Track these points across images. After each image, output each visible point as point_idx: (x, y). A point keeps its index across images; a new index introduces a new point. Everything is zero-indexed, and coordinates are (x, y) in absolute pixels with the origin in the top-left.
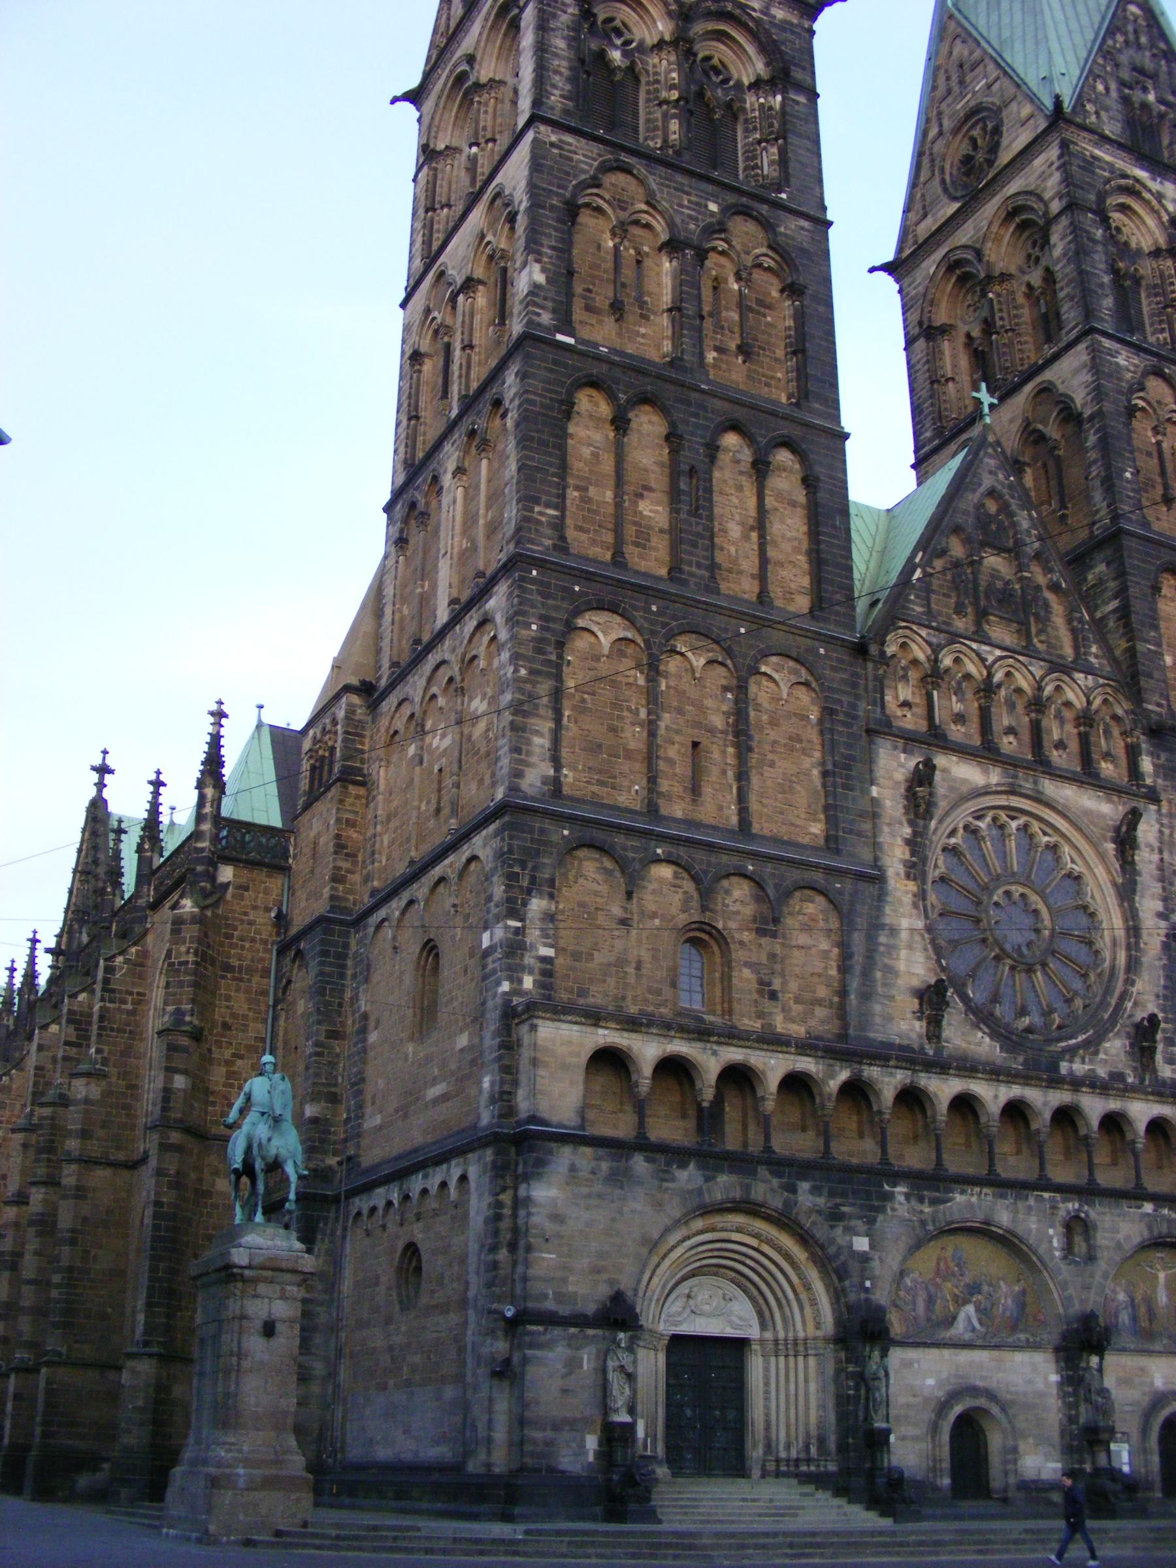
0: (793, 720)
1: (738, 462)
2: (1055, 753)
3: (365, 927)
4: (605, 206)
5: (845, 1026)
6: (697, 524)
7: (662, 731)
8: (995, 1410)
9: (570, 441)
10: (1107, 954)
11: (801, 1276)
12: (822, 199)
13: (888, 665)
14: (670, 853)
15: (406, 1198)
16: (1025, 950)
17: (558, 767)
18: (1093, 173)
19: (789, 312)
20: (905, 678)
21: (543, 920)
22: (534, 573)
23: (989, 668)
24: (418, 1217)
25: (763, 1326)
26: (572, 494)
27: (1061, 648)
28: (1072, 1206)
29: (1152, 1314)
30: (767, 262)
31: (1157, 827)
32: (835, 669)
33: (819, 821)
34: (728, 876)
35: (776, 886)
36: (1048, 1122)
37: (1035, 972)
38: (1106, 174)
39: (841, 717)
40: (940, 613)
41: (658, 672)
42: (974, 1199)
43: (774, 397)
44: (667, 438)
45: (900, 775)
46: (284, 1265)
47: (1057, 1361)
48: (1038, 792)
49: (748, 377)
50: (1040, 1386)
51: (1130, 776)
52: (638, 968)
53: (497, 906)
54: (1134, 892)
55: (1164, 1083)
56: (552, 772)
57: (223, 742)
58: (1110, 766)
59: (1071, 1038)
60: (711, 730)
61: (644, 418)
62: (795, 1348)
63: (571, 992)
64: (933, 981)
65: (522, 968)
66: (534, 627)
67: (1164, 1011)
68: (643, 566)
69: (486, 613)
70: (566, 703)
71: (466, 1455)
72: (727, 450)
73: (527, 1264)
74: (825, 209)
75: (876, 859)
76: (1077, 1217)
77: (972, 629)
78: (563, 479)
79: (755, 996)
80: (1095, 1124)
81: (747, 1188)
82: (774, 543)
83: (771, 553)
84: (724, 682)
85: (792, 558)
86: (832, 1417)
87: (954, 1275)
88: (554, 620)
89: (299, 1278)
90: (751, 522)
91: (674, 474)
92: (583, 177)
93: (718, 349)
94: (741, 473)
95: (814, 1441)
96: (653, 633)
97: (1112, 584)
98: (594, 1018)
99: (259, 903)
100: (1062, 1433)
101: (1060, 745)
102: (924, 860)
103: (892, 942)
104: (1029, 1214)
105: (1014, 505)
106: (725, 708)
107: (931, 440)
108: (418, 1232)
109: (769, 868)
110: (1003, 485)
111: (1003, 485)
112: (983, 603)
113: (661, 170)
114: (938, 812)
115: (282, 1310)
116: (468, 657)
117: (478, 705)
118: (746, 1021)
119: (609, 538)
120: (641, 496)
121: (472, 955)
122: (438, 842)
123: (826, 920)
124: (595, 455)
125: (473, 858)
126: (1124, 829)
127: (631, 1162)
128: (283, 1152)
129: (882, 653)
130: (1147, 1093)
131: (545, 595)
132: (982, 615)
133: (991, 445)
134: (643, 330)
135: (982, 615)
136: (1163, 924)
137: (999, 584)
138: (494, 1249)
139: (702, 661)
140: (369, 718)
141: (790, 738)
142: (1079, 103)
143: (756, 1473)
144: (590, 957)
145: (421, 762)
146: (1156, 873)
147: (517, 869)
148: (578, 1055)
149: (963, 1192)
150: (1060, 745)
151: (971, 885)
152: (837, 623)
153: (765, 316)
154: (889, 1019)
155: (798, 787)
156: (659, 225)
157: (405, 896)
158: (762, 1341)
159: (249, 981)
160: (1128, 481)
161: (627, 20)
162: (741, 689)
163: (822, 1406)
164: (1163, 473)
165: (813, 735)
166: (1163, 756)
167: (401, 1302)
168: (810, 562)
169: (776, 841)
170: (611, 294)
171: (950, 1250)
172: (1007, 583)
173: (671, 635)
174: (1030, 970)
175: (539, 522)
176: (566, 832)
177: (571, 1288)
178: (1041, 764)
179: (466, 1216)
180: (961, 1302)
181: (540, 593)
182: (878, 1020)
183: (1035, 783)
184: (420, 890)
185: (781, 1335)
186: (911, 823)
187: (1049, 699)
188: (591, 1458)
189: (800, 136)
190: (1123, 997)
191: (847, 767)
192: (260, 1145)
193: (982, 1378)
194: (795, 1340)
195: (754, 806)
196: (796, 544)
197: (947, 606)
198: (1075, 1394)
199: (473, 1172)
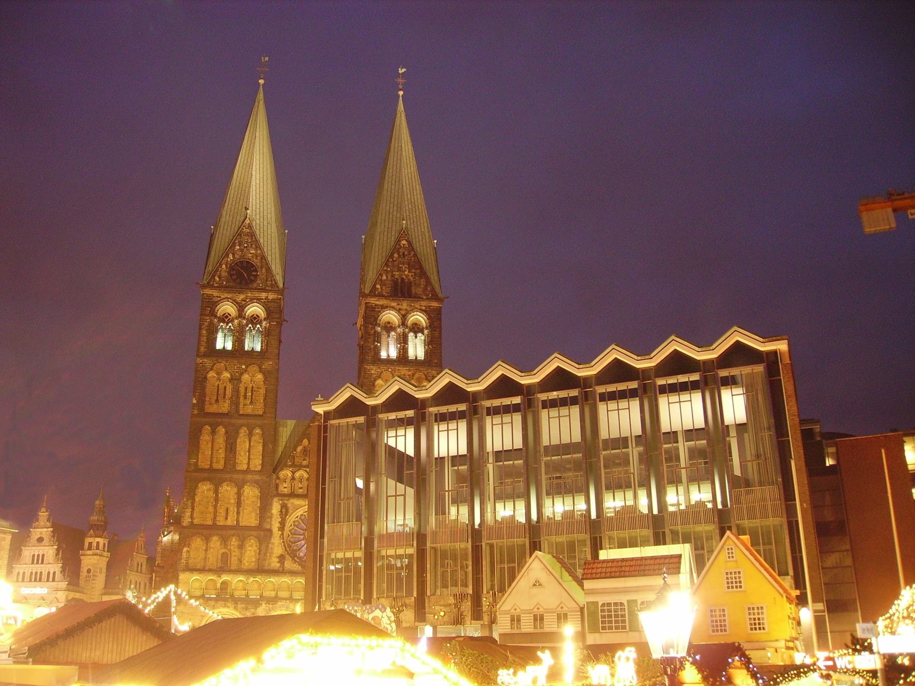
40: (298, 462)
42: (284, 603)
45: (279, 507)
83: (251, 457)
91: (226, 442)
102: (284, 526)
103: (273, 547)
119: (209, 463)
129: (278, 478)
144: (198, 559)
195: (240, 520)
197: (301, 460)
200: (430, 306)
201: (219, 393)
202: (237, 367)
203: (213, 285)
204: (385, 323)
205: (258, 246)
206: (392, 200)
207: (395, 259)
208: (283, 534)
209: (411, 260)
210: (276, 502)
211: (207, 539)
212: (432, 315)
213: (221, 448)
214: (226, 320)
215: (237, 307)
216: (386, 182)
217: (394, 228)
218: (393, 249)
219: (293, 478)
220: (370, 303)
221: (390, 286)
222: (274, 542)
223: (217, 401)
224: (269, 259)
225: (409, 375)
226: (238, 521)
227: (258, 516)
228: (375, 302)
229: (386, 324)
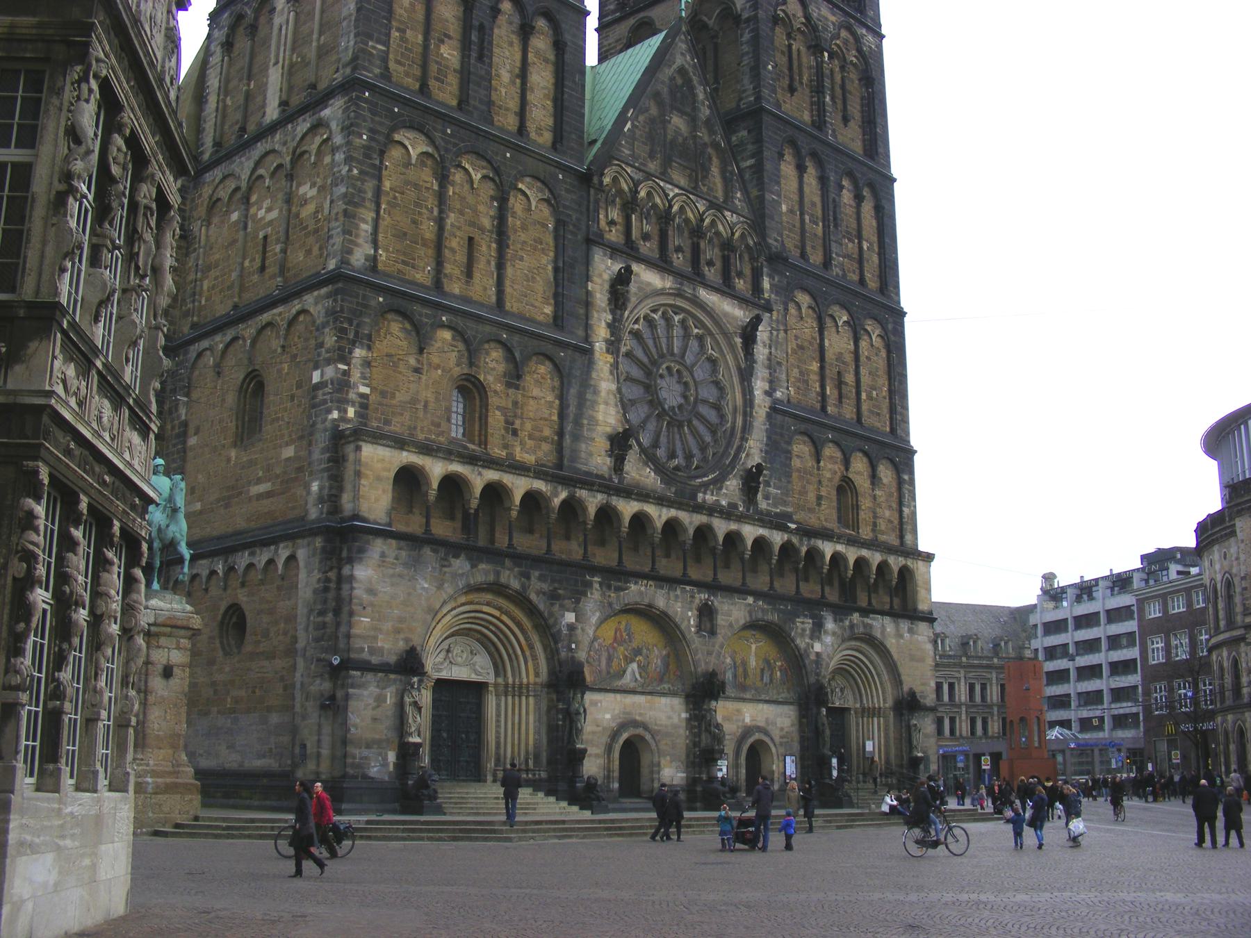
3: (186, 353)
6: (481, 68)
7: (448, 227)
8: (648, 737)
11: (527, 638)
15: (231, 569)
17: (376, 250)
21: (362, 365)
22: (367, 94)
24: (243, 585)
25: (497, 674)
28: (703, 596)
29: (746, 675)
32: (567, 191)
34: (488, 342)
36: (691, 537)
37: (683, 427)
46: (179, 623)
47: (687, 703)
48: (695, 296)
50: (676, 720)
51: (753, 291)
52: (426, 406)
53: (327, 352)
55: (761, 513)
56: (372, 252)
59: (704, 476)
60: (482, 229)
62: (519, 690)
64: (621, 430)
66: (365, 137)
67: (765, 462)
69: (321, 119)
70: (384, 199)
71: (295, 766)
73: (350, 625)
76: (706, 604)
78: (390, 22)
79: (503, 432)
80: (721, 539)
81: (498, 574)
86: (545, 741)
87: (625, 641)
89: (190, 633)
90: (517, 71)
95: (531, 757)
96: (447, 150)
97: (750, 147)
98: (400, 443)
100: (688, 756)
102: (619, 340)
104: (676, 601)
105: (695, 80)
106: (492, 213)
107: (614, 12)
108: (242, 597)
110: (689, 64)
111: (689, 64)
114: (630, 306)
115: (177, 657)
116: (298, 151)
117: (307, 190)
118: (496, 450)
119: (417, 71)
120: (442, 42)
121: (299, 386)
122: (262, 293)
123: (552, 379)
125: (303, 311)
126: (749, 329)
127: (422, 552)
128: (178, 535)
130: (755, 520)
131: (374, 113)
132: (667, 163)
135: (667, 163)
136: (768, 399)
137: (680, 139)
138: (322, 613)
139: (479, 176)
140: (191, 185)
143: (490, 778)
145: (245, 228)
146: (766, 362)
147: (345, 325)
148: (389, 470)
149: (636, 583)
151: (645, 360)
154: (590, 454)
155: (538, 278)
157: (230, 334)
158: (496, 685)
160: (769, 72)
163: (537, 732)
164: (790, 68)
165: (549, 240)
167: (223, 649)
168: (555, 106)
169: (521, 317)
171: (624, 623)
173: (459, 154)
174: (680, 426)
175: (371, 54)
176: (381, 299)
177: (379, 644)
179: (295, 586)
180: (629, 660)
181: (370, 111)
182: (583, 455)
184: (248, 330)
185: (510, 681)
186: (612, 312)
188: (391, 768)
190: (740, 449)
192: (159, 530)
193: (640, 714)
194: (521, 684)
195: (508, 290)
196: (546, 92)
198: (699, 726)
199: (301, 554)
211: (421, 339)
213: (449, 37)
226: (500, 292)
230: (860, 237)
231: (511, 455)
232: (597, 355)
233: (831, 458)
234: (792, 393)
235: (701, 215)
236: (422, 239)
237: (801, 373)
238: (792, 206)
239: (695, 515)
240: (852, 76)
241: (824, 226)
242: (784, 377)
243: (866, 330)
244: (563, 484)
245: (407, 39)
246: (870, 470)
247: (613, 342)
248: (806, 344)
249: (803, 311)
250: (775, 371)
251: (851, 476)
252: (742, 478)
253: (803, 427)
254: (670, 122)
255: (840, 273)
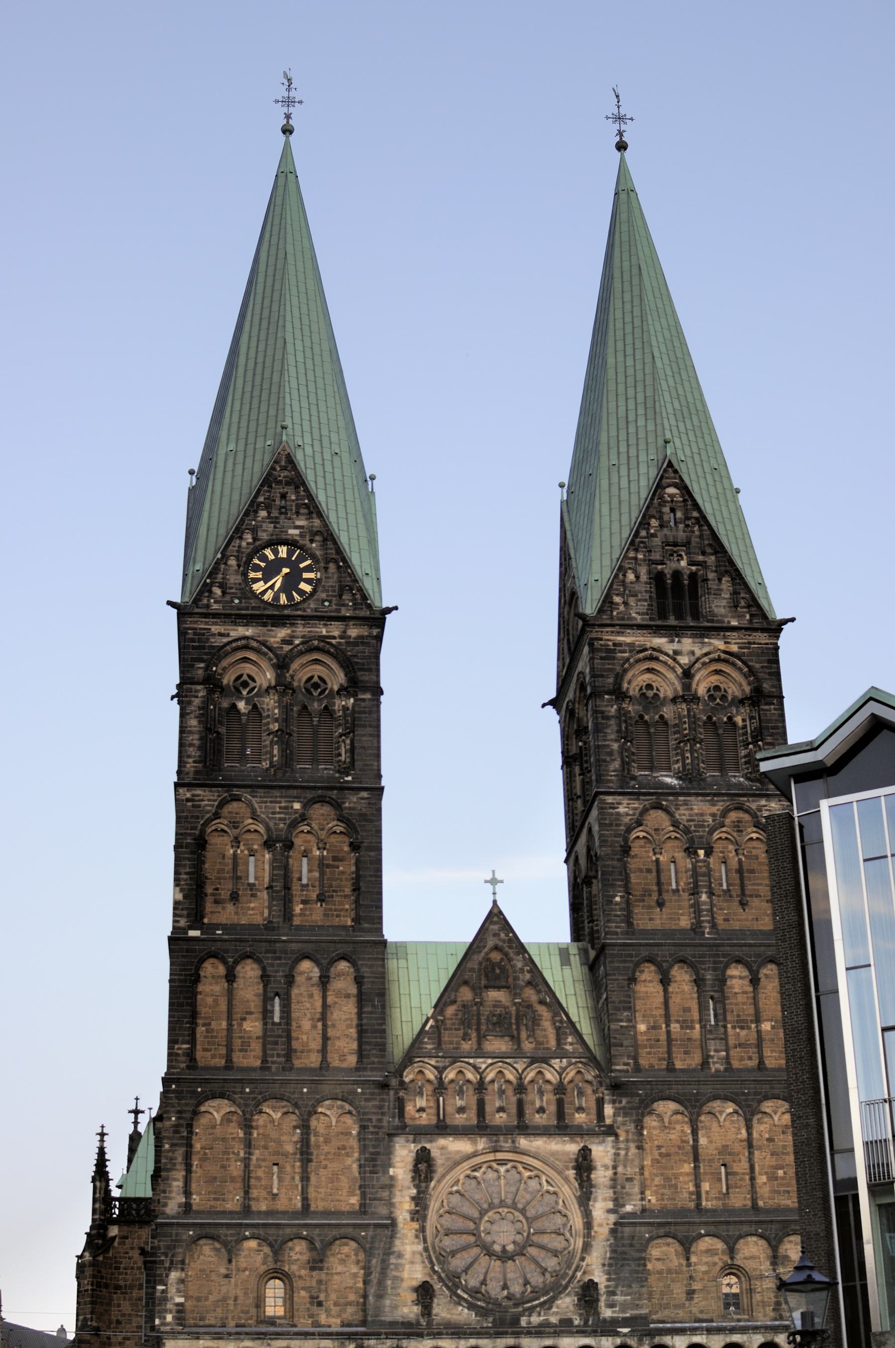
0: (341, 1136)
1: (310, 979)
2: (537, 1116)
4: (226, 828)
5: (365, 1316)
9: (199, 997)
10: (572, 1241)
12: (379, 770)
13: (405, 1089)
14: (254, 1233)
16: (510, 1248)
18: (614, 658)
19: (353, 861)
20: (421, 1094)
23: (481, 1074)
26: (201, 1030)
27: (547, 1042)
30: (338, 829)
31: (613, 1151)
32: (366, 1100)
33: (356, 1195)
34: (291, 1240)
35: (322, 1241)
38: (626, 655)
39: (371, 1129)
40: (451, 1043)
41: (251, 1127)
43: (341, 924)
44: (262, 976)
49: (325, 915)
52: (236, 1299)
54: (589, 1199)
55: (605, 1320)
56: (184, 1200)
57: (106, 1150)
58: (583, 1116)
60: (286, 1155)
61: (248, 968)
63: (196, 1319)
65: (166, 1311)
66: (173, 1119)
67: (609, 1273)
68: (245, 1063)
72: (302, 973)
74: (379, 777)
75: (391, 1213)
77: (475, 1046)
79: (308, 1306)
82: (334, 1026)
83: (331, 1033)
84: (294, 1123)
85: (347, 1032)
88: (185, 1111)
90: (318, 1016)
91: (266, 1000)
92: (208, 816)
93: (304, 902)
94: (313, 985)
99: (135, 1245)
101: (542, 1110)
102: (426, 1208)
106: (296, 1138)
109: (317, 1231)
110: (504, 941)
112: (484, 1027)
113: (261, 791)
114: (436, 1176)
118: (302, 1321)
119: (223, 1051)
120: (244, 1019)
123: (356, 1255)
124: (216, 1001)
129: (402, 1083)
133: (496, 915)
134: (252, 905)
135: (481, 1038)
137: (498, 1011)
139: (279, 1114)
141: (339, 1149)
142: (607, 602)
144: (207, 1299)
147: (163, 1258)
150: (542, 1110)
152: (372, 1069)
153: (338, 867)
154: (395, 1307)
155: (342, 1178)
156: (261, 828)
159: (131, 1293)
160: (617, 904)
161: (253, 674)
162: (305, 1127)
164: (659, 883)
165: (354, 1143)
166: (624, 1101)
169: (327, 1213)
170: (231, 887)
172: (505, 1008)
173: (259, 1104)
175: (177, 1055)
176: (191, 1233)
178: (523, 1128)
181: (176, 1097)
182: (387, 1309)
183: (513, 1142)
186: (416, 1186)
187: (532, 1081)
189: (365, 726)
190: (578, 1268)
191: (374, 1160)
196: (349, 1022)
197: (457, 1036)
200: (749, 643)
201: (239, 874)
202: (280, 808)
203: (208, 606)
204: (641, 689)
205: (313, 509)
206: (631, 392)
207: (652, 531)
208: (423, 1229)
209: (693, 532)
210: (404, 1147)
211: (231, 1251)
212: (758, 666)
213: (250, 1013)
214: (245, 692)
215: (270, 659)
216: (610, 351)
217: (643, 457)
218: (648, 507)
219: (440, 1087)
220: (601, 639)
221: (647, 596)
222: (401, 1248)
223: (235, 897)
224: (343, 539)
225: (713, 815)
226: (305, 1199)
227: (357, 1185)
228: (612, 638)
229: (644, 691)
230: (758, 1020)
231: (316, 1324)
232: (400, 1225)
233: (708, 1251)
234: (654, 1200)
235: (521, 1075)
236: (231, 1177)
237: (667, 1179)
238: (655, 1022)
239: (499, 1340)
240: (754, 852)
241: (701, 1028)
242: (636, 1190)
243: (765, 1113)
244: (349, 1339)
245: (213, 1030)
246: (769, 1252)
247: (417, 1212)
248: (673, 1150)
249: (666, 1120)
250: (623, 1187)
251: (736, 1263)
252: (577, 1294)
253: (661, 1231)
254: (481, 1003)
255: (722, 1068)
